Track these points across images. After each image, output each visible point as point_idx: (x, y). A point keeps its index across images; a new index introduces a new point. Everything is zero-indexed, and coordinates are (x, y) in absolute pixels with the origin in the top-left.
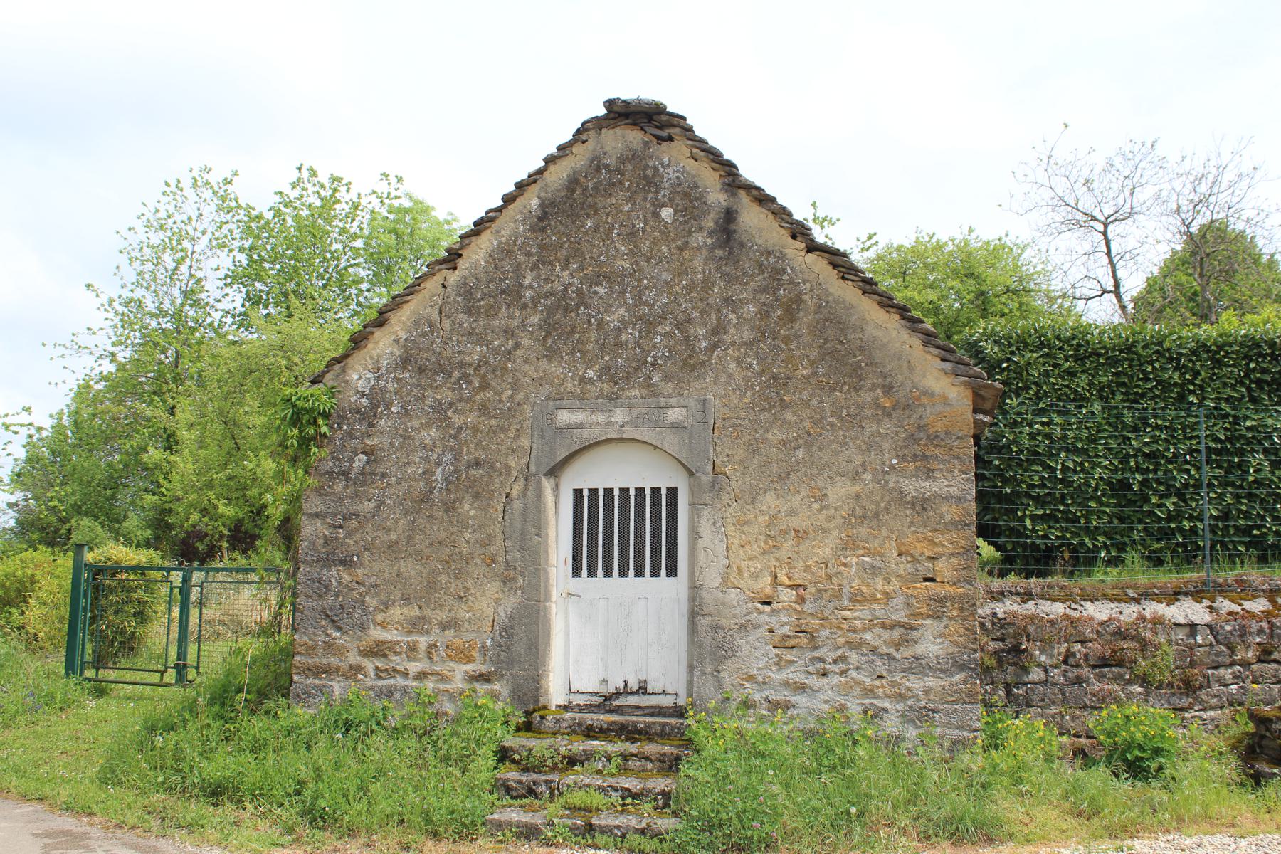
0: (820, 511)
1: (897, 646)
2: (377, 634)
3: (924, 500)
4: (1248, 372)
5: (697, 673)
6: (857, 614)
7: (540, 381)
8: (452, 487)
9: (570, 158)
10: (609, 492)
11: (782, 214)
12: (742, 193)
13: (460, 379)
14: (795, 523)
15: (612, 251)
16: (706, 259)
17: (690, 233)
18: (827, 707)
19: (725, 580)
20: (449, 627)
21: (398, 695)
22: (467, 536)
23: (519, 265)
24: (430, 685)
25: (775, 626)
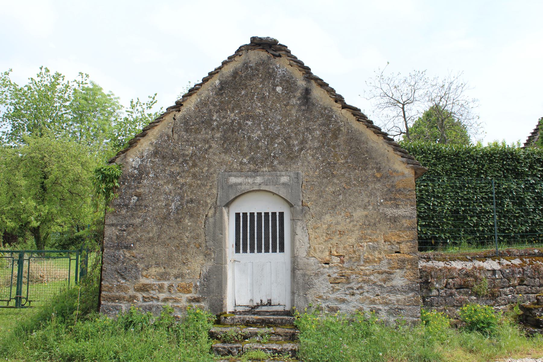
0: (350, 222)
1: (385, 281)
2: (143, 281)
3: (395, 218)
4: (503, 165)
5: (296, 295)
6: (367, 267)
7: (221, 163)
8: (179, 212)
9: (234, 62)
10: (252, 214)
11: (331, 91)
12: (313, 82)
13: (183, 162)
14: (339, 228)
15: (254, 105)
16: (297, 110)
17: (290, 98)
18: (354, 309)
19: (308, 253)
20: (179, 277)
21: (154, 309)
22: (187, 234)
23: (210, 111)
24: (169, 304)
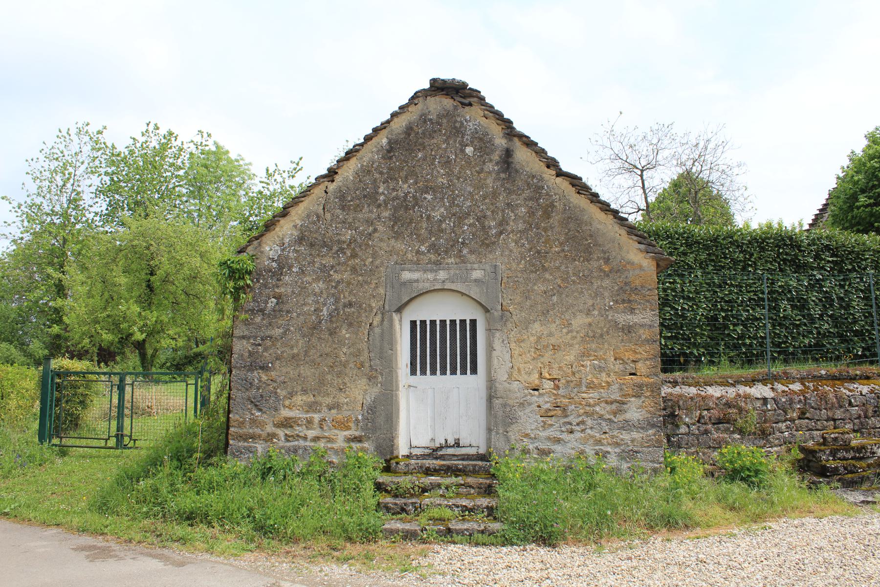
0: (567, 333)
1: (615, 414)
2: (285, 413)
3: (630, 327)
4: (779, 254)
5: (493, 433)
7: (391, 253)
8: (334, 319)
10: (433, 322)
12: (516, 139)
13: (338, 251)
14: (553, 341)
15: (435, 172)
16: (495, 179)
17: (484, 163)
18: (573, 452)
19: (510, 375)
20: (333, 408)
21: (300, 452)
22: (345, 350)
24: (321, 444)
25: (541, 404)
